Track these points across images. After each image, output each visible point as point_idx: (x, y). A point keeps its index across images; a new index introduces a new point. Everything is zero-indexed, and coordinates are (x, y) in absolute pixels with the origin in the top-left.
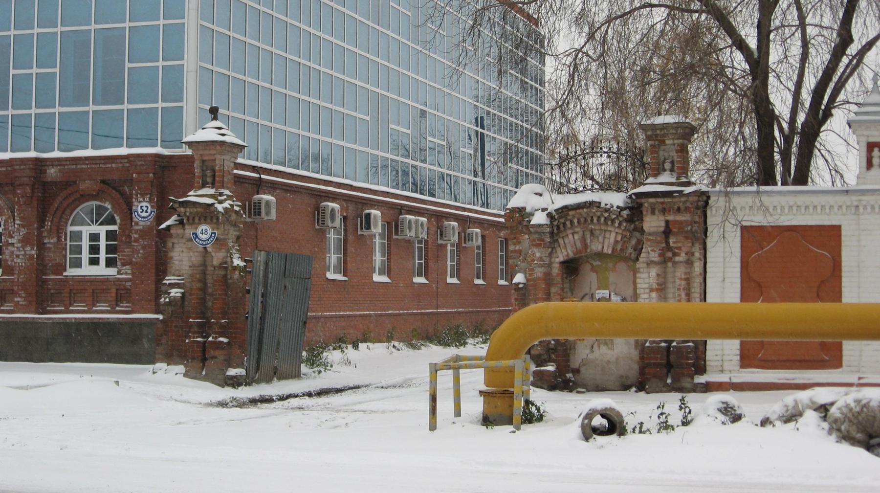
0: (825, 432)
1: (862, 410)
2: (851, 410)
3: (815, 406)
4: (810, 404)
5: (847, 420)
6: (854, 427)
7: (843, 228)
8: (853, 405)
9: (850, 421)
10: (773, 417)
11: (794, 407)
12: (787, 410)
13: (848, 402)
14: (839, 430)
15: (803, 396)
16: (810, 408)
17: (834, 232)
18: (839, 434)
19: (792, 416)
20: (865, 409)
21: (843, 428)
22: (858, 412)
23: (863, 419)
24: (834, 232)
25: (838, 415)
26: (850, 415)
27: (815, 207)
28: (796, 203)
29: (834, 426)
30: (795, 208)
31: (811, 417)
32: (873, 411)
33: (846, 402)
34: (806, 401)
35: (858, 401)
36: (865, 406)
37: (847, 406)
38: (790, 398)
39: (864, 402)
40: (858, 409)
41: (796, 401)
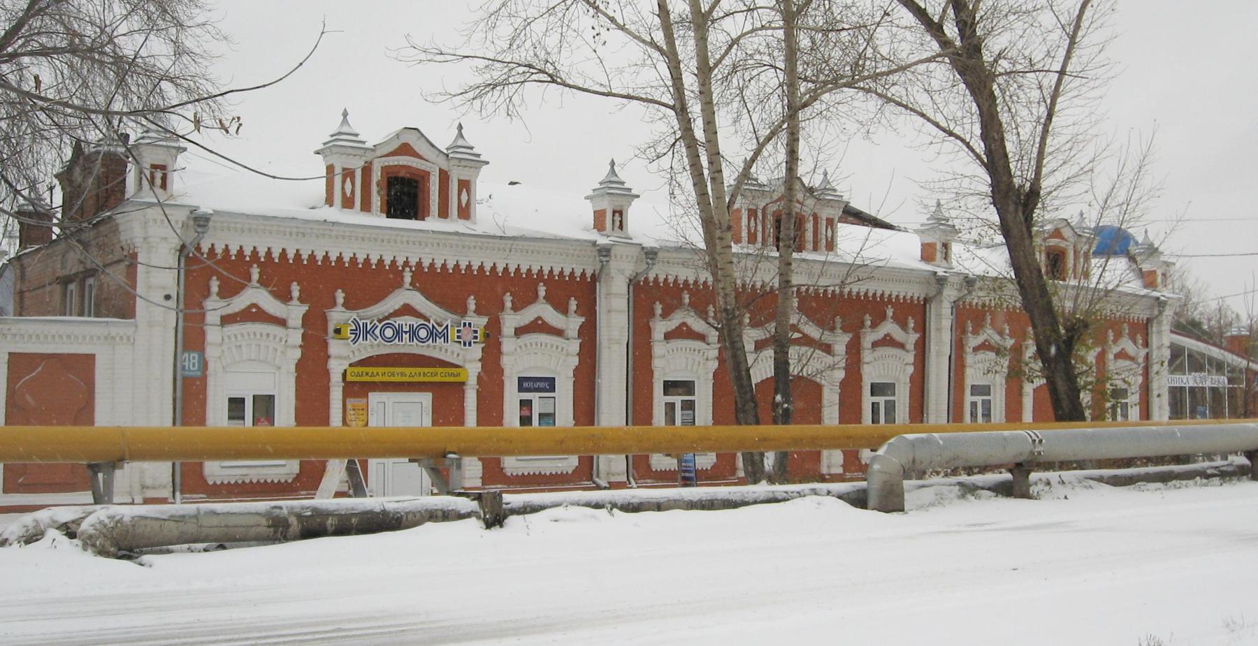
0: (80, 548)
1: (116, 525)
2: (105, 526)
3: (56, 526)
4: (50, 522)
5: (102, 536)
6: (109, 542)
7: (97, 357)
8: (107, 521)
9: (105, 536)
10: (12, 538)
11: (34, 527)
12: (27, 531)
13: (102, 518)
14: (94, 545)
15: (43, 515)
16: (53, 527)
17: (90, 358)
18: (94, 549)
19: (32, 537)
20: (119, 525)
21: (98, 543)
22: (112, 528)
23: (117, 534)
24: (90, 358)
25: (92, 531)
26: (105, 531)
27: (61, 337)
28: (118, 334)
29: (88, 542)
30: (34, 337)
31: (53, 533)
32: (127, 526)
33: (99, 519)
34: (47, 521)
35: (111, 517)
36: (118, 522)
37: (101, 522)
38: (28, 519)
39: (117, 518)
40: (112, 525)
41: (36, 521)
